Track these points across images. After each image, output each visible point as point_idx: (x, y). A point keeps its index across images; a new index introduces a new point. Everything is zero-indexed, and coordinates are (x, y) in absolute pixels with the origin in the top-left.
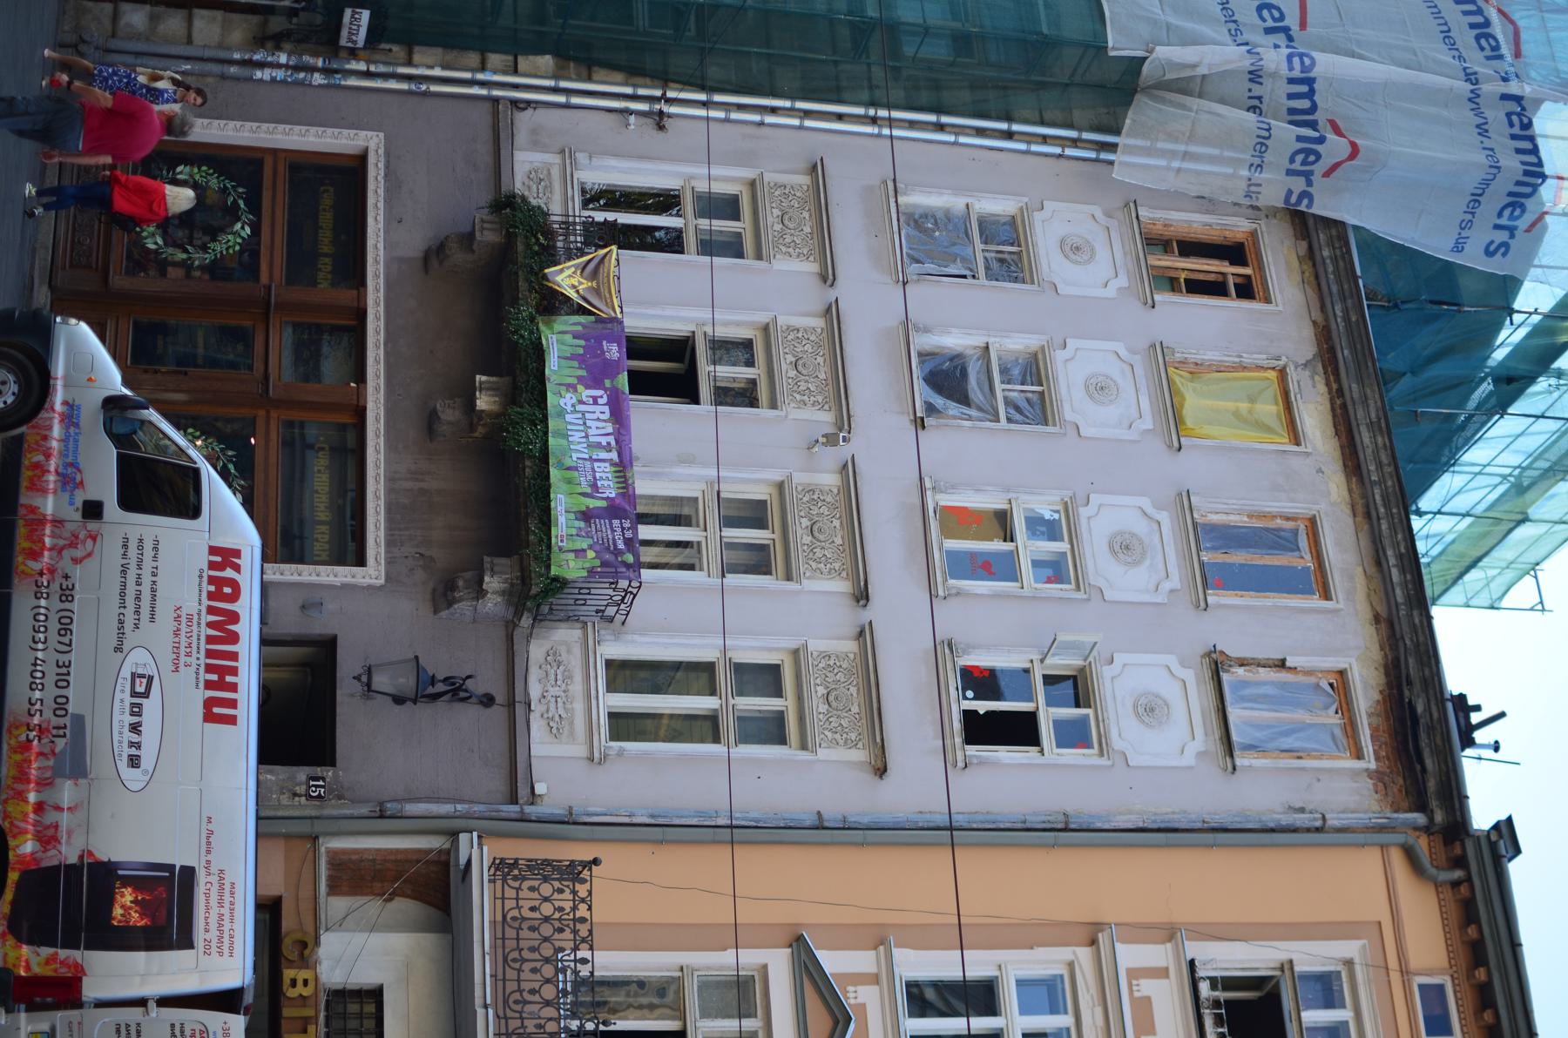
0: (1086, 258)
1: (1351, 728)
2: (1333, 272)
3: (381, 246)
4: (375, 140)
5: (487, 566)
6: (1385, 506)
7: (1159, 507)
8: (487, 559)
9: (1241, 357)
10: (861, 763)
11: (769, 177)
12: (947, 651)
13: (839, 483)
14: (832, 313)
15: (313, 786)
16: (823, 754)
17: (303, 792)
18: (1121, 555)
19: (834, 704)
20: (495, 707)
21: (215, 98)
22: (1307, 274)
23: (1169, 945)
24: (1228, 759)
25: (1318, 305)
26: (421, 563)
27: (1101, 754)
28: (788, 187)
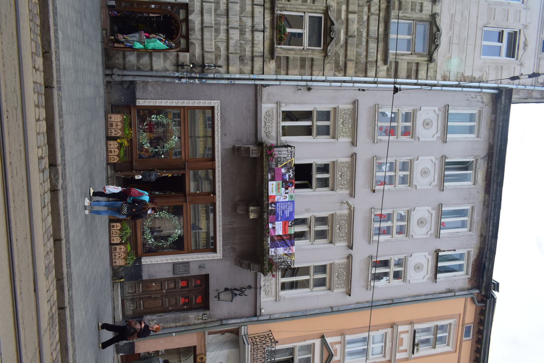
0: (430, 127)
3: (219, 145)
7: (433, 209)
8: (252, 266)
10: (344, 292)
11: (341, 106)
14: (353, 156)
17: (201, 318)
19: (339, 278)
21: (163, 90)
23: (410, 326)
26: (232, 250)
28: (346, 110)
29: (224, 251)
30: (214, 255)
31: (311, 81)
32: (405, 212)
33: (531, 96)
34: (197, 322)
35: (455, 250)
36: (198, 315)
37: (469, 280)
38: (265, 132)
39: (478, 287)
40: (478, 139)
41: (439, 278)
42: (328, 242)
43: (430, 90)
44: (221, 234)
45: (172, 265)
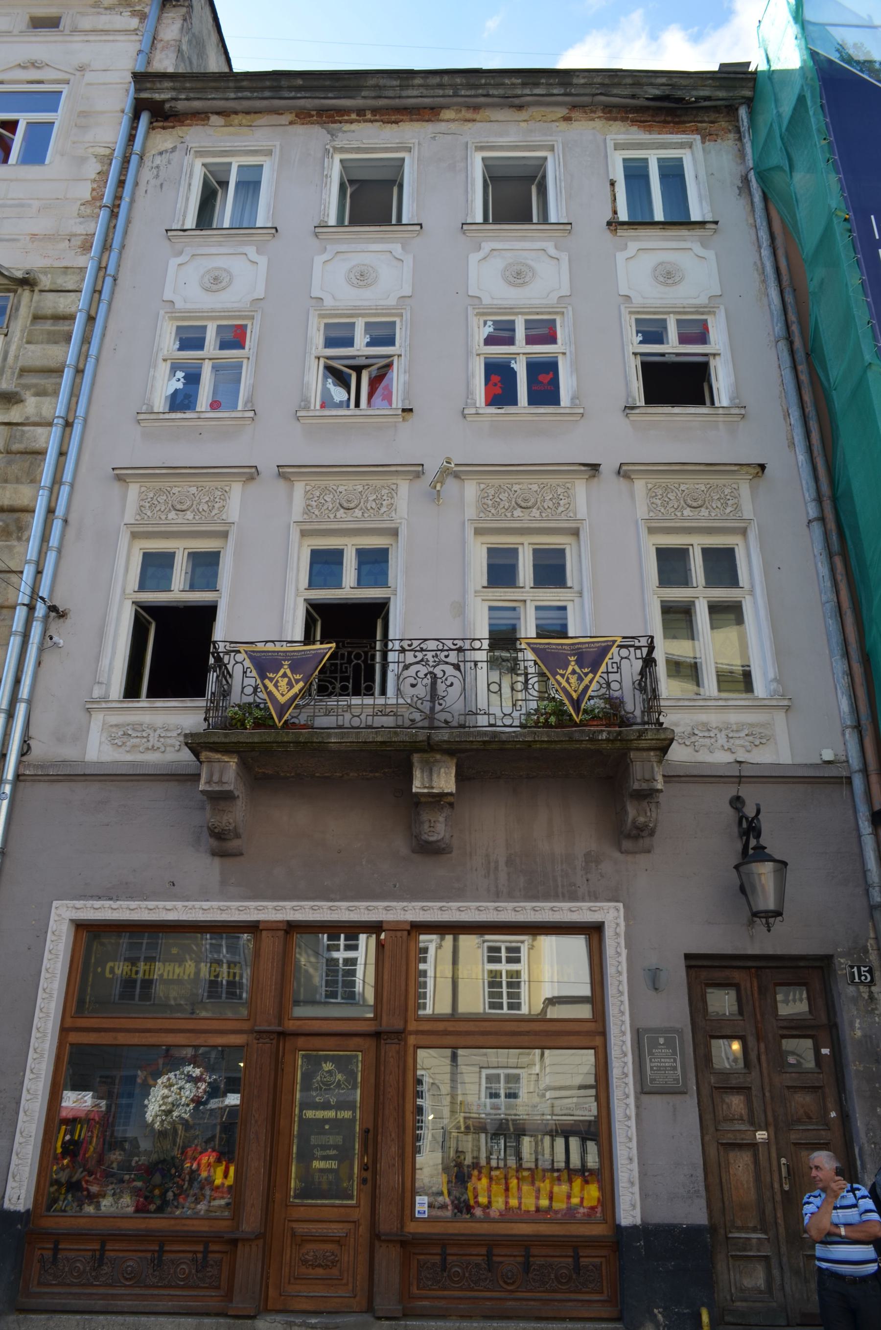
2: (251, 92)
3: (206, 905)
5: (645, 786)
6: (478, 89)
7: (480, 248)
8: (636, 786)
10: (751, 487)
11: (130, 516)
12: (637, 411)
15: (860, 978)
18: (527, 279)
19: (700, 502)
20: (740, 794)
22: (244, 121)
26: (593, 865)
27: (714, 313)
28: (142, 503)
29: (594, 897)
30: (609, 932)
31: (31, 608)
33: (172, 43)
35: (613, 184)
37: (709, 140)
38: (178, 751)
39: (731, 110)
40: (277, 152)
41: (704, 216)
43: (115, 280)
44: (529, 905)
45: (645, 1098)
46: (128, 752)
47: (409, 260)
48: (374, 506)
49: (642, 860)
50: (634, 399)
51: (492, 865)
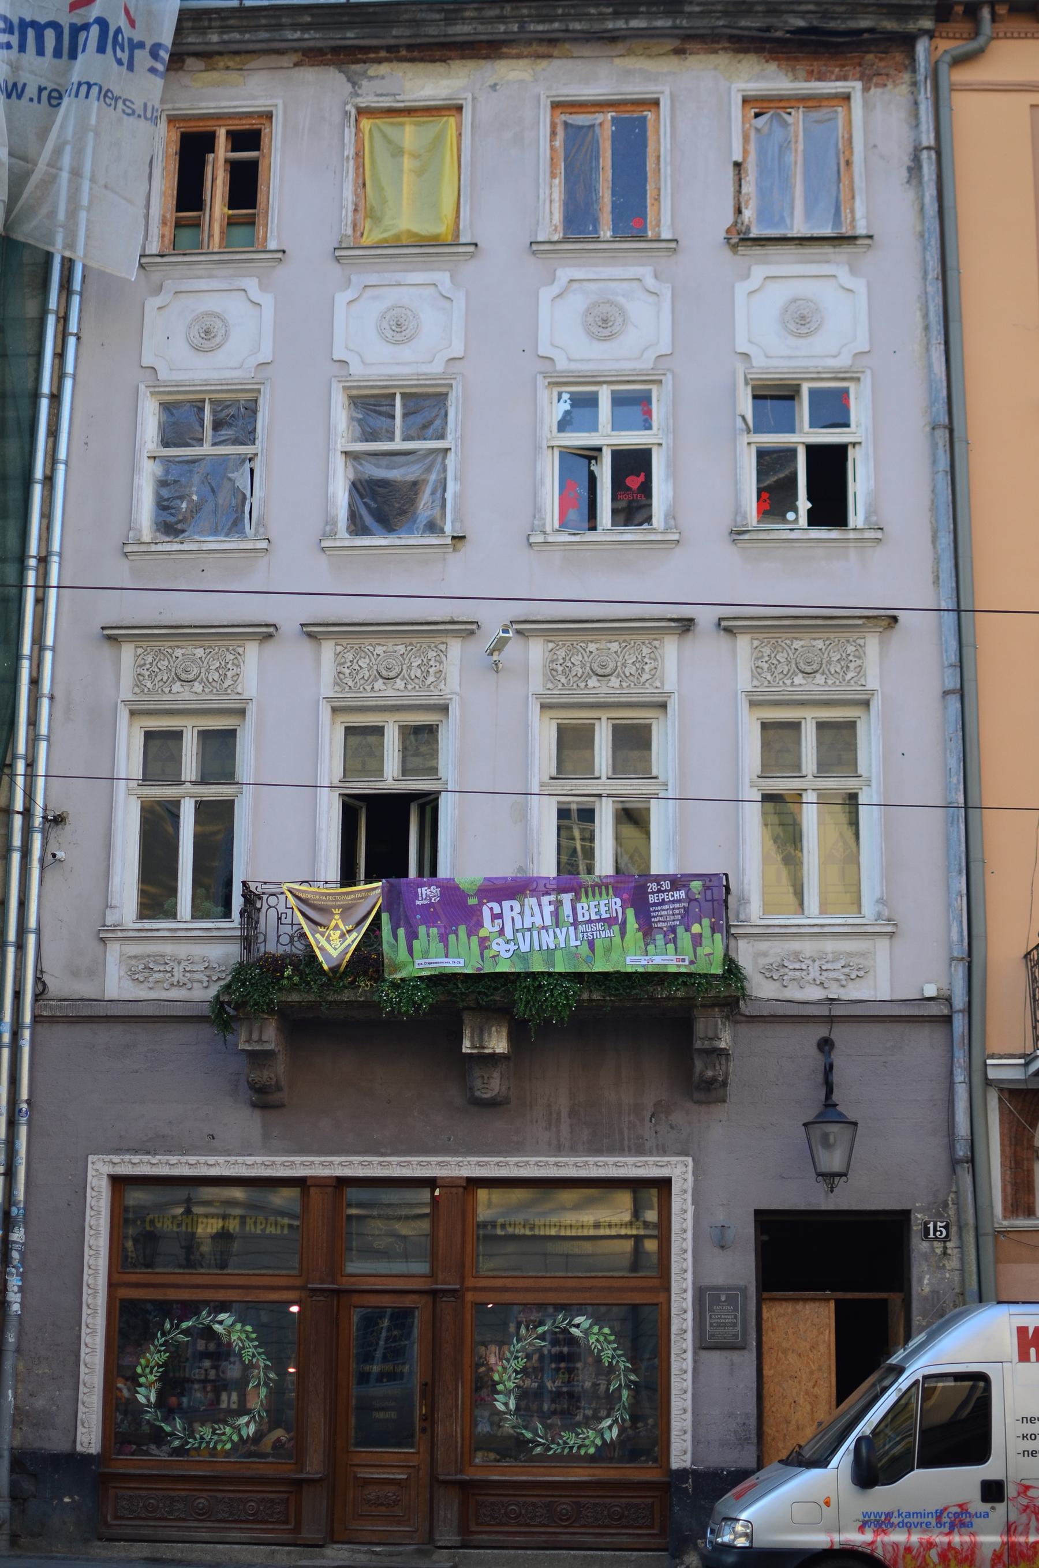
0: (219, 324)
1: (810, 102)
2: (241, 33)
3: (250, 1160)
4: (99, 1165)
5: (707, 1045)
6: (552, 21)
9: (348, 157)
10: (881, 643)
11: (126, 692)
12: (746, 537)
13: (541, 640)
15: (934, 1234)
16: (872, 682)
18: (616, 329)
19: (815, 667)
20: (833, 1037)
24: (859, 242)
25: (274, 57)
26: (663, 1116)
27: (858, 379)
28: (140, 670)
32: (559, 401)
34: (953, 1263)
36: (926, 1257)
37: (877, 85)
38: (206, 987)
42: (662, 717)
43: (78, 339)
44: (591, 1160)
45: (705, 1355)
46: (151, 988)
47: (460, 299)
48: (419, 674)
49: (719, 1111)
50: (745, 518)
51: (554, 1116)
